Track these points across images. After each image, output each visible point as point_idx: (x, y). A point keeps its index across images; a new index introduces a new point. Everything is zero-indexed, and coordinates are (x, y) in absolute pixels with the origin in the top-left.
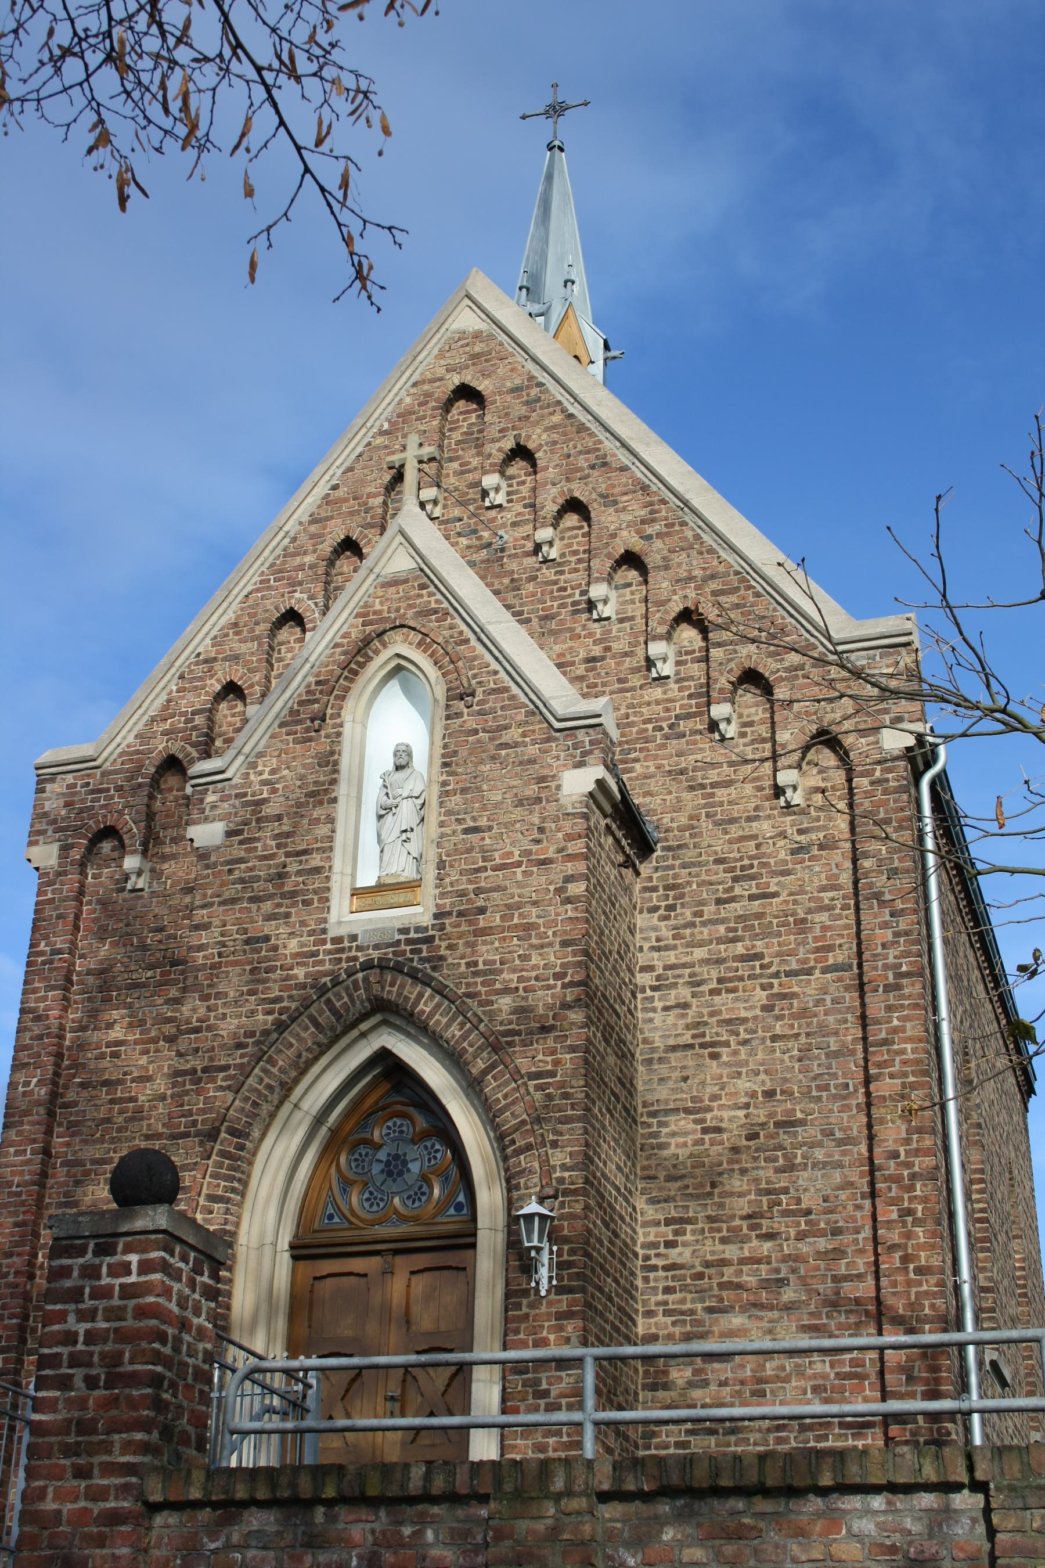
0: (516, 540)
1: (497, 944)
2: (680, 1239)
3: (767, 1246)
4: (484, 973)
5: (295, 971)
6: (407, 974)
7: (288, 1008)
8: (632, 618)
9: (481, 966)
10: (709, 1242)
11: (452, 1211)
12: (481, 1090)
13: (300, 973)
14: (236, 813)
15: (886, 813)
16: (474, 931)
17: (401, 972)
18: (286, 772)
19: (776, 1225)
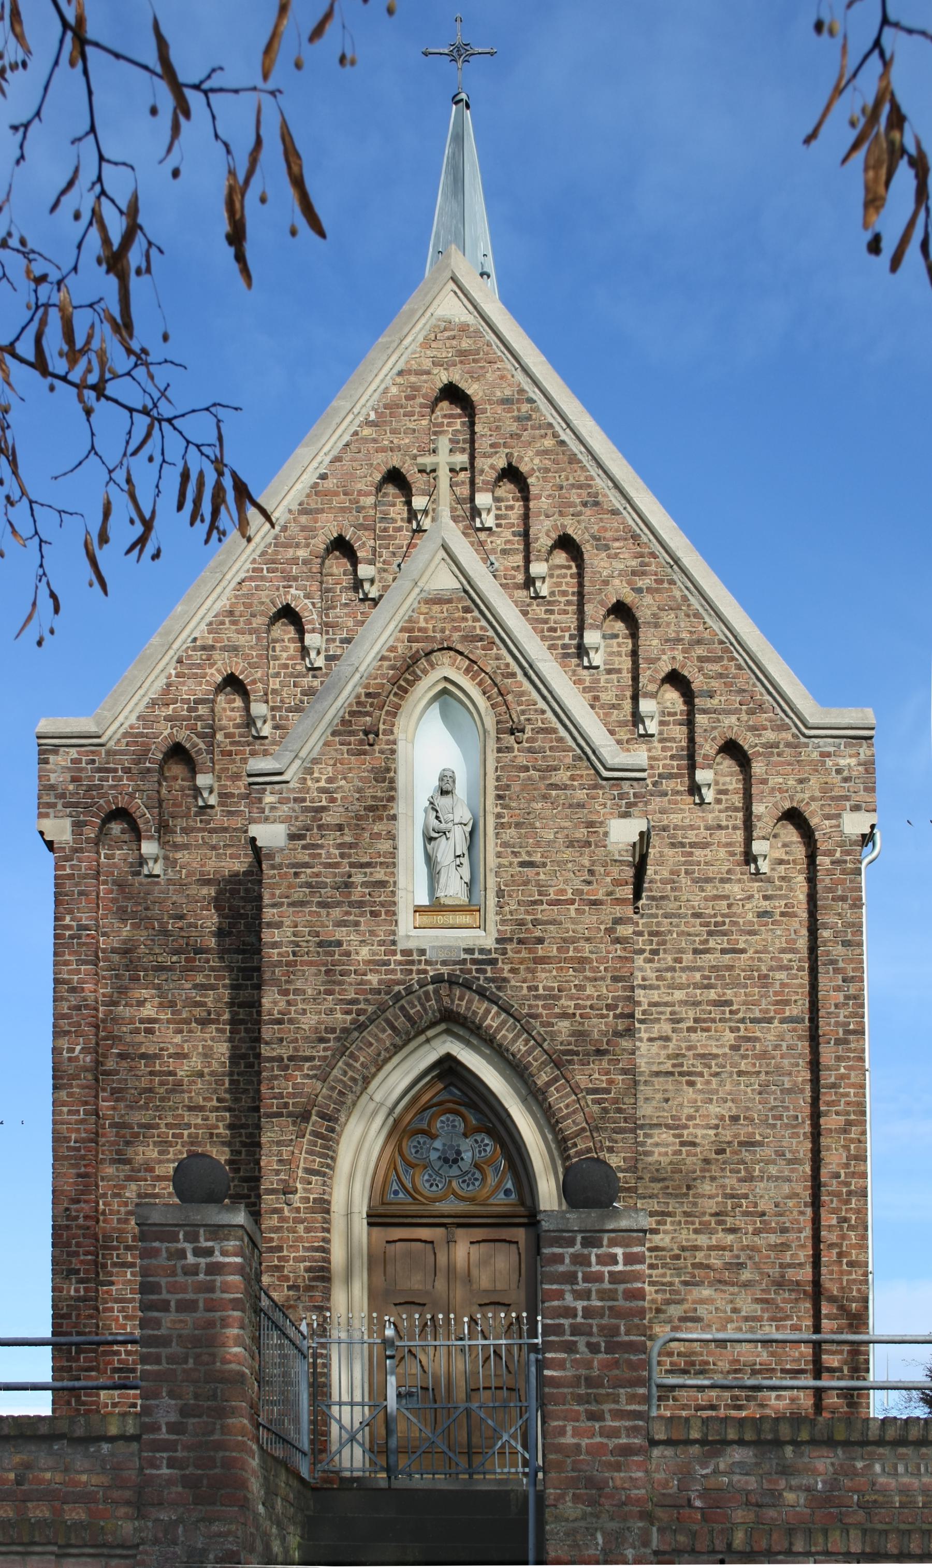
0: (506, 569)
1: (554, 973)
2: (661, 1228)
3: (730, 1238)
4: (545, 998)
5: (369, 977)
6: (475, 991)
7: (365, 1011)
8: (619, 671)
9: (541, 991)
10: (685, 1232)
11: (502, 1195)
12: (545, 1099)
13: (373, 979)
14: (297, 818)
15: (843, 891)
16: (534, 958)
17: (470, 989)
18: (343, 783)
19: (737, 1222)
